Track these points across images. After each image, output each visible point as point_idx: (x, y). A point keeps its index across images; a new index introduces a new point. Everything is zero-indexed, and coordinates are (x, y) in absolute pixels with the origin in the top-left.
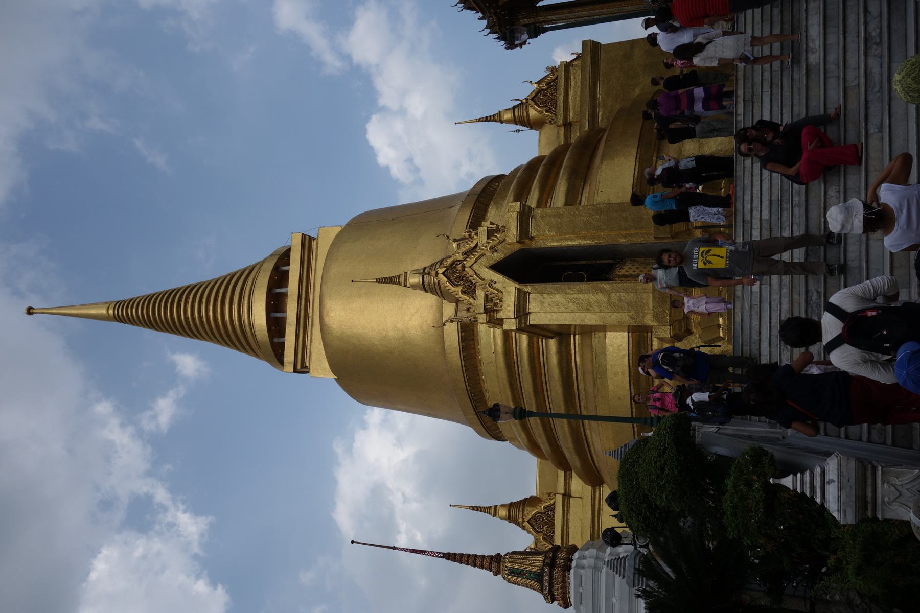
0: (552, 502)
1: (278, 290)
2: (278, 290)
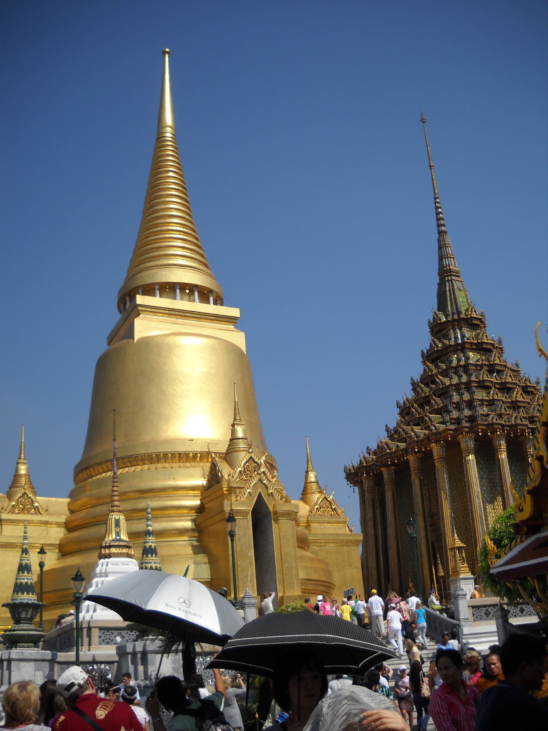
0: (41, 512)
1: (196, 293)
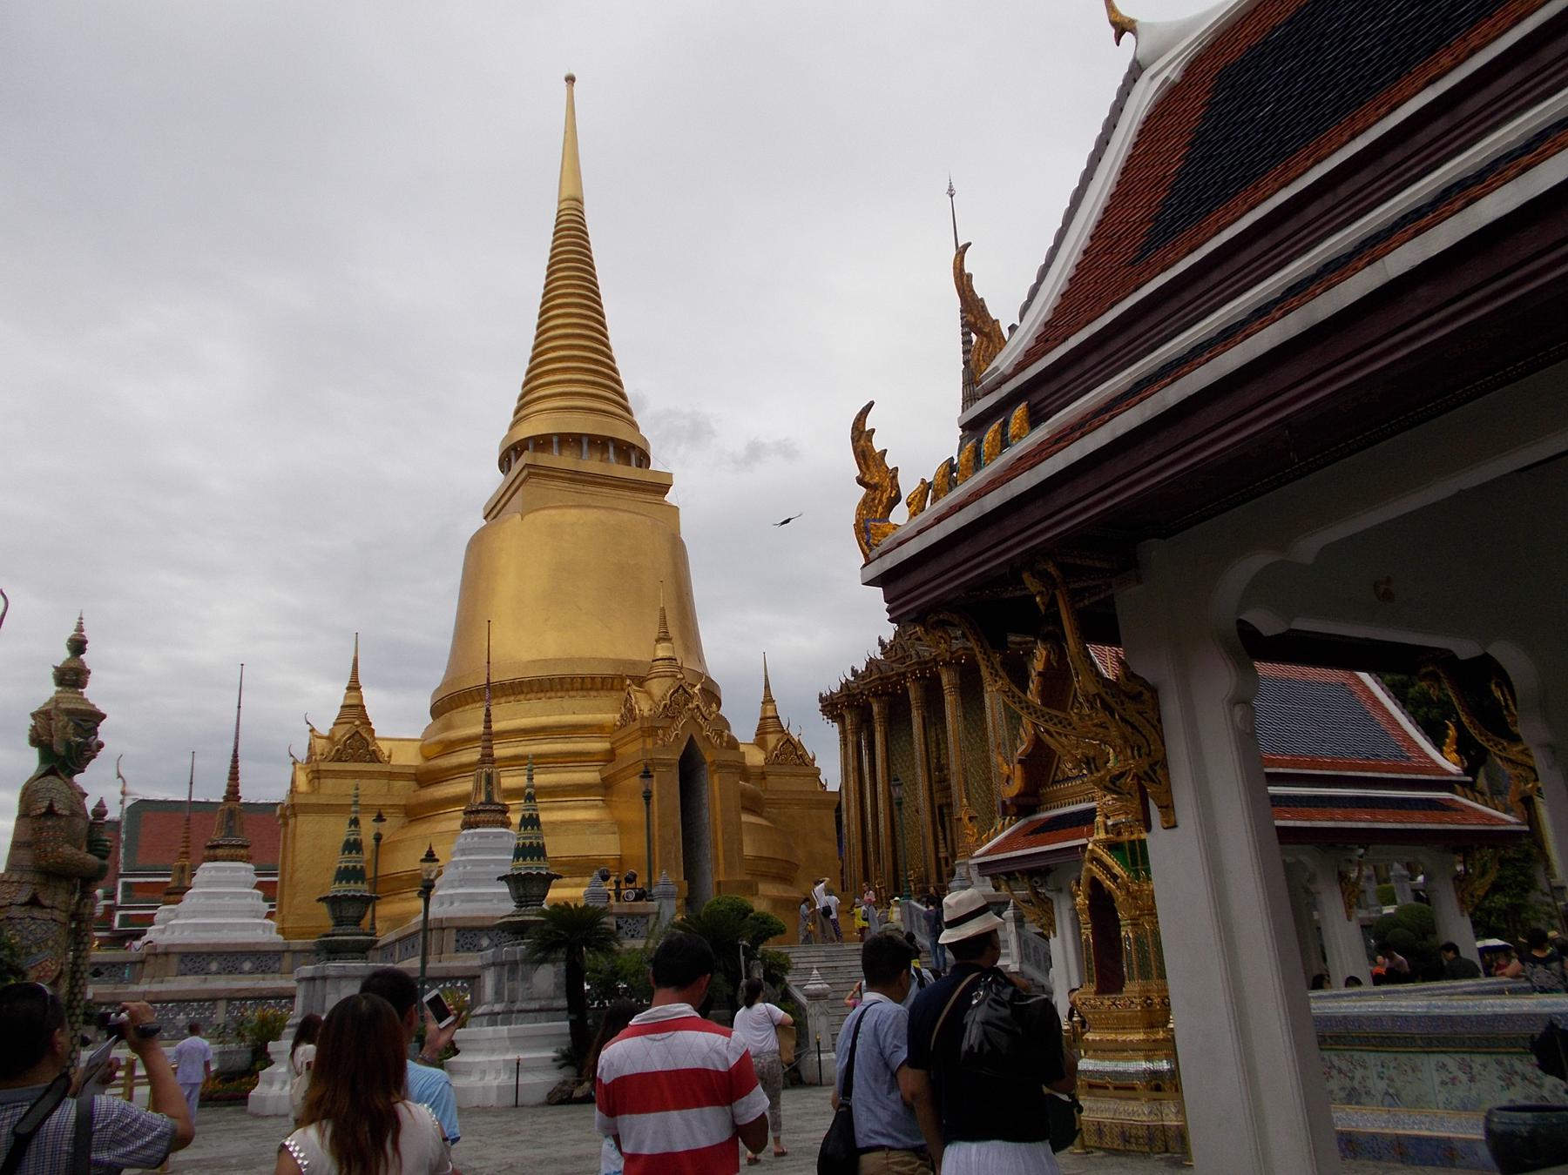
1: (611, 449)
2: (611, 449)
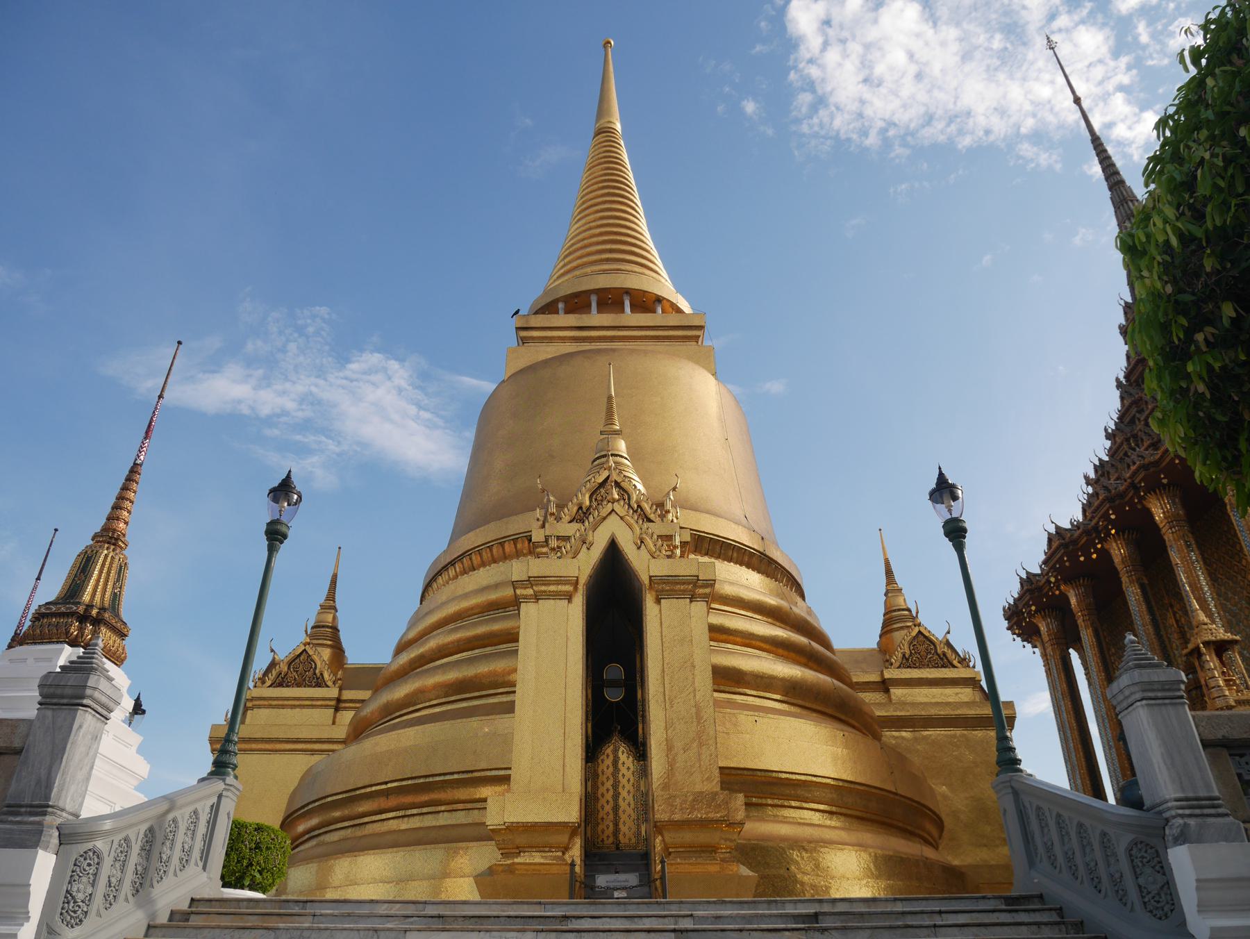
0: (329, 683)
